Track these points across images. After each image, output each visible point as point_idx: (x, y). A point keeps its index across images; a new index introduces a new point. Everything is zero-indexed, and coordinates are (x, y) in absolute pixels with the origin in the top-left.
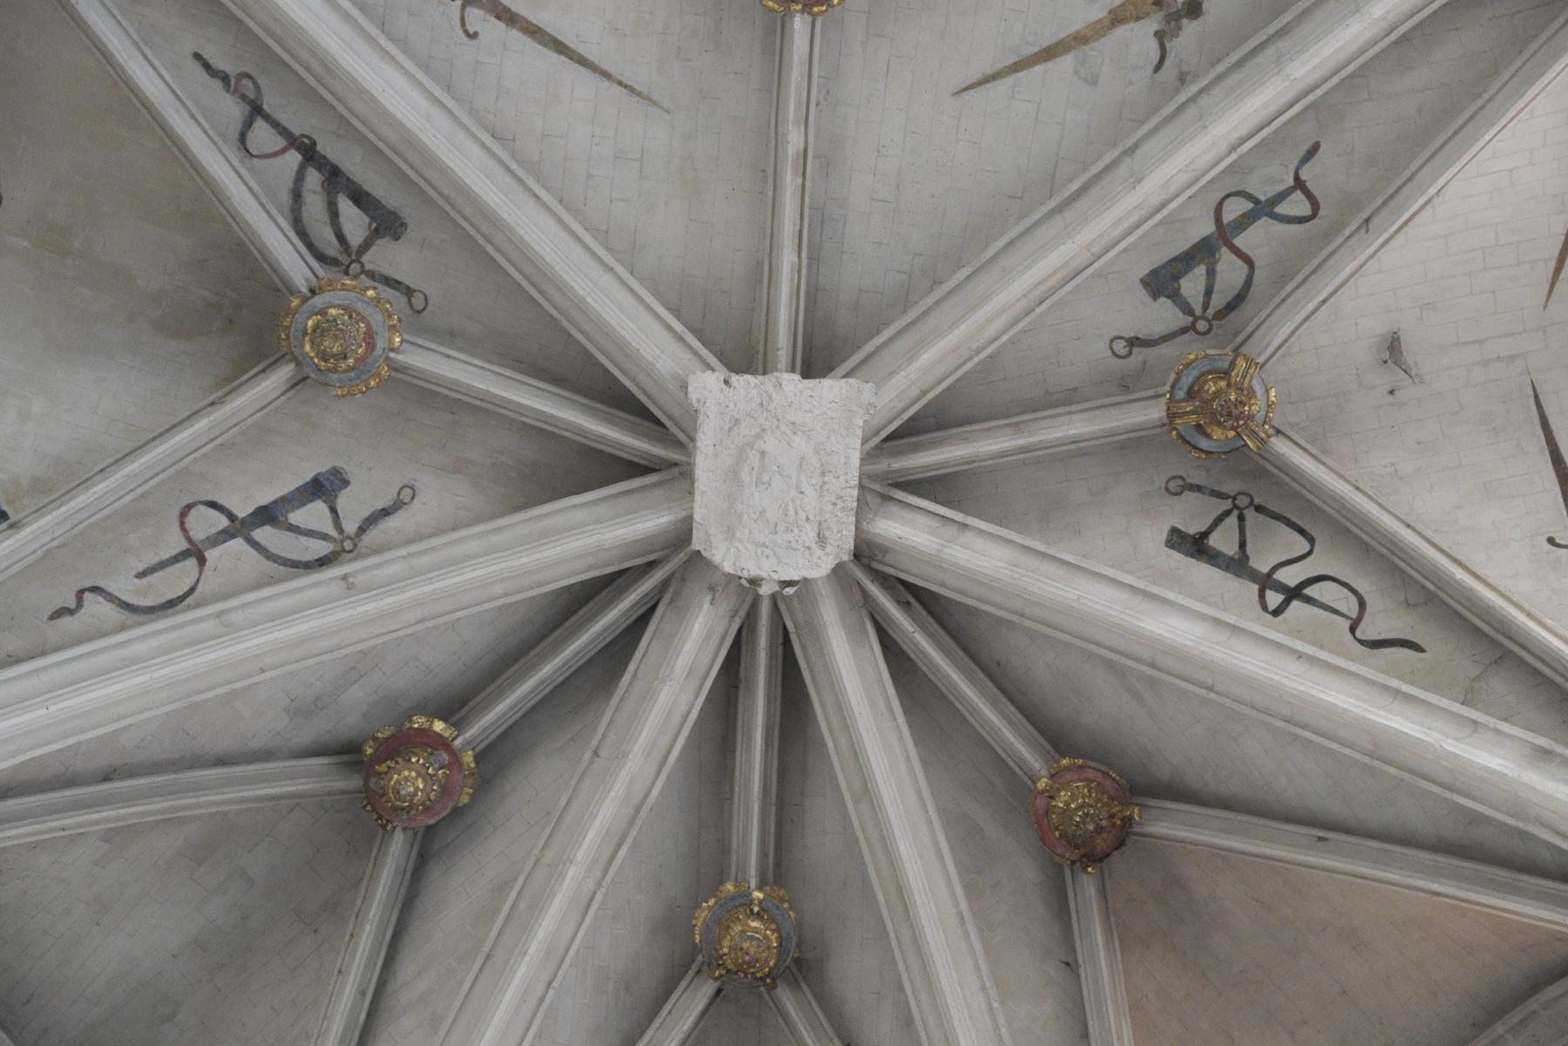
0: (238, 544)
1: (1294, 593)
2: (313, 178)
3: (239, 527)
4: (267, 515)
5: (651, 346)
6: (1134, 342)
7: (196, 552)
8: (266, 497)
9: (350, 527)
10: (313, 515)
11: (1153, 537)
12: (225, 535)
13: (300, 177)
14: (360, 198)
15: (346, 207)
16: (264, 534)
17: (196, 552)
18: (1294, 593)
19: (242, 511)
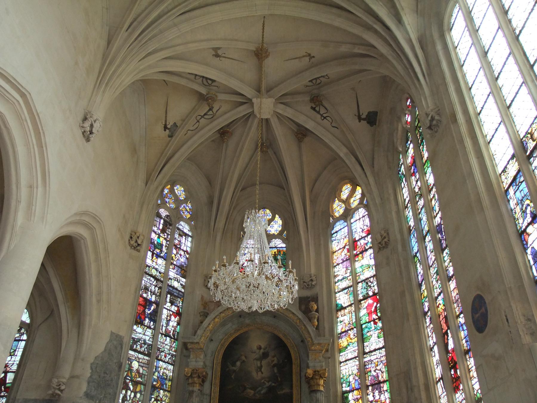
0: (203, 119)
2: (204, 79)
3: (202, 117)
4: (205, 114)
5: (248, 92)
6: (307, 86)
7: (198, 121)
8: (205, 112)
9: (215, 112)
10: (211, 112)
11: (309, 108)
12: (201, 118)
13: (202, 81)
14: (210, 79)
15: (208, 81)
16: (206, 117)
17: (198, 121)
19: (202, 115)
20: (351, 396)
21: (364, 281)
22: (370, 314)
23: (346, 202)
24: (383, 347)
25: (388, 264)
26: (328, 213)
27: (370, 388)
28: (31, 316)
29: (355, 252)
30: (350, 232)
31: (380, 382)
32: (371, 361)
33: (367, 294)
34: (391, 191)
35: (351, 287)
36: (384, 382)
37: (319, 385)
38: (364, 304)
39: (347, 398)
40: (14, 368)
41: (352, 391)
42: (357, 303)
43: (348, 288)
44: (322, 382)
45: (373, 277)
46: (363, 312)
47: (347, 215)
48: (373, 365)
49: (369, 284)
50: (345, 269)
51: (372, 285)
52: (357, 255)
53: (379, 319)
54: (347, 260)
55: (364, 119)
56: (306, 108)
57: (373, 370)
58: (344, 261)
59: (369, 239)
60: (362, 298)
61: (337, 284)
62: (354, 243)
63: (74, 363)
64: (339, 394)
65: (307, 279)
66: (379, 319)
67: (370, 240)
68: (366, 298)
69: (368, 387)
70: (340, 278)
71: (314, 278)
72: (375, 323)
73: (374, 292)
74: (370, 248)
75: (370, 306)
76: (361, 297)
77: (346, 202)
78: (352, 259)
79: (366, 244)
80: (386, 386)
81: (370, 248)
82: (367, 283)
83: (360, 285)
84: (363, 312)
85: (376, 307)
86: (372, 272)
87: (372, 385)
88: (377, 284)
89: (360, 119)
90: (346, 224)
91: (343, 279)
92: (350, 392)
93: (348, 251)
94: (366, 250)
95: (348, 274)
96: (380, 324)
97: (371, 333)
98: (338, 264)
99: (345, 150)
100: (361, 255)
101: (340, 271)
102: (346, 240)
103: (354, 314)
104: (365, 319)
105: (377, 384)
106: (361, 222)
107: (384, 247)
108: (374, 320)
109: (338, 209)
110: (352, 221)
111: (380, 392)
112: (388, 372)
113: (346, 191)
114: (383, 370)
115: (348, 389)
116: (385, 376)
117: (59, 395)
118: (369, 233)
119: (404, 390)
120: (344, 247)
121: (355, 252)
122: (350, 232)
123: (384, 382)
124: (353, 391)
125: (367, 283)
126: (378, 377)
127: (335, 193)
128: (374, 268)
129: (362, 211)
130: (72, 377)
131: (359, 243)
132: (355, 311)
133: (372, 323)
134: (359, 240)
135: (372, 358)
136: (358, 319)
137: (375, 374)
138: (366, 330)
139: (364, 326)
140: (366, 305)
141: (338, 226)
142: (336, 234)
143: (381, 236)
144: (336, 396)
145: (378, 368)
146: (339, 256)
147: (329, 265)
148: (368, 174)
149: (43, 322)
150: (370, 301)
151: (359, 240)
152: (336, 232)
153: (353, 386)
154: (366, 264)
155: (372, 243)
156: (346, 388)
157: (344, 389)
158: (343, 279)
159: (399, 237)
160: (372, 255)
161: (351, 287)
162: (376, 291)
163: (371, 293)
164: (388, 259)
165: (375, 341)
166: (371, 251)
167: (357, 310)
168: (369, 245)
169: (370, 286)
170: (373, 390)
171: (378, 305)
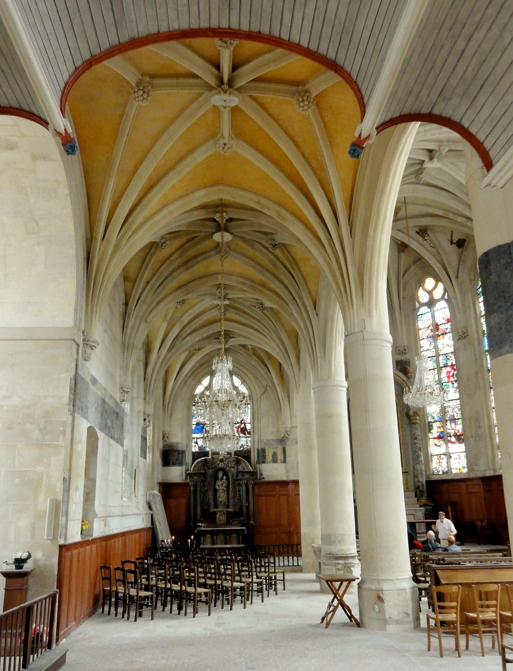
1: (426, 240)
18: (426, 240)
20: (434, 425)
21: (445, 354)
22: (449, 377)
23: (430, 293)
24: (458, 399)
25: (465, 349)
26: (414, 298)
27: (449, 421)
28: (249, 388)
29: (437, 333)
30: (433, 316)
31: (455, 419)
32: (450, 406)
33: (447, 364)
34: (471, 302)
35: (434, 356)
36: (458, 419)
37: (416, 420)
38: (444, 371)
39: (432, 426)
40: (249, 421)
41: (436, 422)
42: (440, 369)
43: (432, 357)
44: (418, 418)
45: (452, 353)
46: (444, 375)
47: (431, 303)
48: (451, 409)
49: (448, 357)
50: (429, 343)
51: (450, 359)
52: (438, 336)
53: (456, 381)
54: (430, 337)
55: (454, 243)
56: (413, 233)
57: (450, 411)
58: (428, 338)
59: (448, 326)
60: (443, 366)
61: (422, 353)
62: (437, 327)
63: (291, 419)
64: (427, 423)
65: (401, 349)
66: (456, 381)
67: (450, 327)
68: (446, 366)
69: (447, 421)
70: (425, 349)
71: (406, 348)
72: (453, 384)
73: (452, 364)
74: (449, 332)
75: (449, 372)
76: (442, 365)
77: (430, 293)
78: (435, 337)
79: (447, 329)
80: (460, 422)
81: (449, 332)
82: (447, 357)
83: (441, 357)
84: (444, 375)
85: (453, 374)
86: (452, 350)
87: (450, 420)
88: (455, 357)
89: (452, 243)
90: (429, 310)
91: (428, 350)
92: (434, 422)
93: (432, 331)
94: (446, 333)
95: (432, 347)
96: (456, 385)
97: (450, 389)
98: (424, 339)
99: (439, 265)
100: (442, 336)
101: (425, 344)
102: (430, 322)
103: (437, 376)
104: (445, 379)
105: (453, 420)
106: (442, 312)
107: (462, 338)
108: (452, 382)
109: (423, 296)
110: (435, 309)
111: (456, 424)
112: (462, 414)
113: (430, 283)
114: (458, 412)
115: (433, 420)
116: (459, 416)
117: (287, 437)
118: (448, 321)
119: (474, 427)
120: (428, 327)
121: (437, 333)
122: (433, 316)
123: (458, 419)
124: (436, 422)
125: (447, 357)
126: (454, 416)
127: (421, 283)
128: (453, 347)
129: (443, 304)
130: (292, 427)
131: (440, 327)
132: (438, 373)
133: (450, 383)
134: (441, 325)
135: (450, 404)
136: (440, 380)
137: (452, 414)
138: (446, 387)
139: (444, 384)
140: (446, 371)
141: (423, 310)
142: (421, 316)
143: (463, 332)
144: (425, 424)
145: (454, 411)
146: (424, 333)
147: (416, 339)
148: (455, 285)
149: (263, 394)
150: (449, 369)
151: (441, 325)
152: (422, 315)
153: (436, 419)
154: (446, 344)
155: (451, 329)
156: (430, 419)
157: (430, 420)
158: (428, 350)
159: (475, 335)
160: (451, 338)
161: (434, 356)
162: (454, 363)
163: (449, 364)
164: (465, 346)
165: (453, 394)
166: (450, 335)
167: (439, 373)
168: (448, 330)
169: (449, 359)
170: (450, 423)
171: (456, 372)
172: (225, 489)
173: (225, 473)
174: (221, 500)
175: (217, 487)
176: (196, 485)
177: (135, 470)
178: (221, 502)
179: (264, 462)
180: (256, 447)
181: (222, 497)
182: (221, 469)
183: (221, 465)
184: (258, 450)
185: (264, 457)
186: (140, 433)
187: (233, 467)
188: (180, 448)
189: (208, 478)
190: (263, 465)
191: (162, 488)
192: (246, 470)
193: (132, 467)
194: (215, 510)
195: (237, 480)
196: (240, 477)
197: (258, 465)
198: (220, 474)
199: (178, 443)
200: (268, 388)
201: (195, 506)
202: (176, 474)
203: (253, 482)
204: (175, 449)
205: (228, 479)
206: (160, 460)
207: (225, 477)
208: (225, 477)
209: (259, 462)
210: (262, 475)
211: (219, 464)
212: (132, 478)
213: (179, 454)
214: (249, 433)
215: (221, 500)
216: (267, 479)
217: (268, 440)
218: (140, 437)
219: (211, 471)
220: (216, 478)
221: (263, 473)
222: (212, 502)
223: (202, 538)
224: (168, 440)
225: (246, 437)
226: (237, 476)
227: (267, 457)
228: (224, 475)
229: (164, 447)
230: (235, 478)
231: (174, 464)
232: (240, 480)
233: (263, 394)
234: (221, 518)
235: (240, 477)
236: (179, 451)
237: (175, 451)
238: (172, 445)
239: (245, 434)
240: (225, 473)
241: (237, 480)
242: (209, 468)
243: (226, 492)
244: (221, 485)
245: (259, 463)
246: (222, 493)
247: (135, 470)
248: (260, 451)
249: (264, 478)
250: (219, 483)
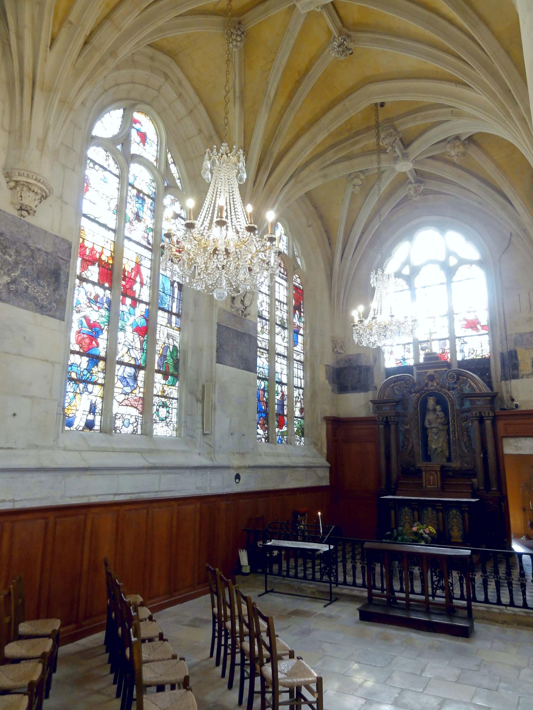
149: (503, 253)
172: (441, 427)
173: (441, 401)
174: (434, 447)
175: (427, 424)
176: (387, 420)
177: (203, 387)
178: (436, 449)
179: (515, 377)
180: (499, 350)
181: (437, 443)
182: (431, 394)
183: (433, 386)
184: (502, 354)
185: (516, 367)
186: (215, 320)
187: (453, 389)
188: (363, 362)
189: (411, 410)
190: (513, 381)
191: (330, 426)
192: (478, 391)
193: (197, 380)
194: (426, 464)
195: (463, 412)
196: (467, 405)
197: (503, 382)
198: (431, 402)
199: (358, 355)
200: (514, 239)
201: (388, 458)
202: (356, 405)
203: (491, 414)
204: (354, 365)
205: (445, 410)
206: (327, 382)
207: (438, 407)
208: (438, 407)
209: (505, 377)
210: (513, 400)
211: (427, 385)
212: (198, 401)
213: (360, 372)
214: (483, 327)
215: (434, 447)
216: (523, 408)
217: (521, 335)
218: (215, 327)
219: (414, 397)
220: (424, 410)
221: (514, 396)
222: (419, 450)
223: (393, 512)
224: (342, 352)
225: (480, 335)
226: (462, 405)
227: (521, 368)
228: (437, 403)
229: (338, 363)
230: (458, 407)
231: (354, 389)
232: (468, 411)
233: (503, 253)
234: (432, 480)
235: (467, 405)
236: (360, 367)
237: (355, 368)
238: (350, 360)
239: (476, 329)
240: (441, 401)
241: (463, 412)
242: (411, 393)
243: (444, 433)
244: (433, 419)
245: (506, 379)
246: (436, 434)
247: (203, 387)
248: (506, 355)
249: (517, 406)
250: (430, 416)
